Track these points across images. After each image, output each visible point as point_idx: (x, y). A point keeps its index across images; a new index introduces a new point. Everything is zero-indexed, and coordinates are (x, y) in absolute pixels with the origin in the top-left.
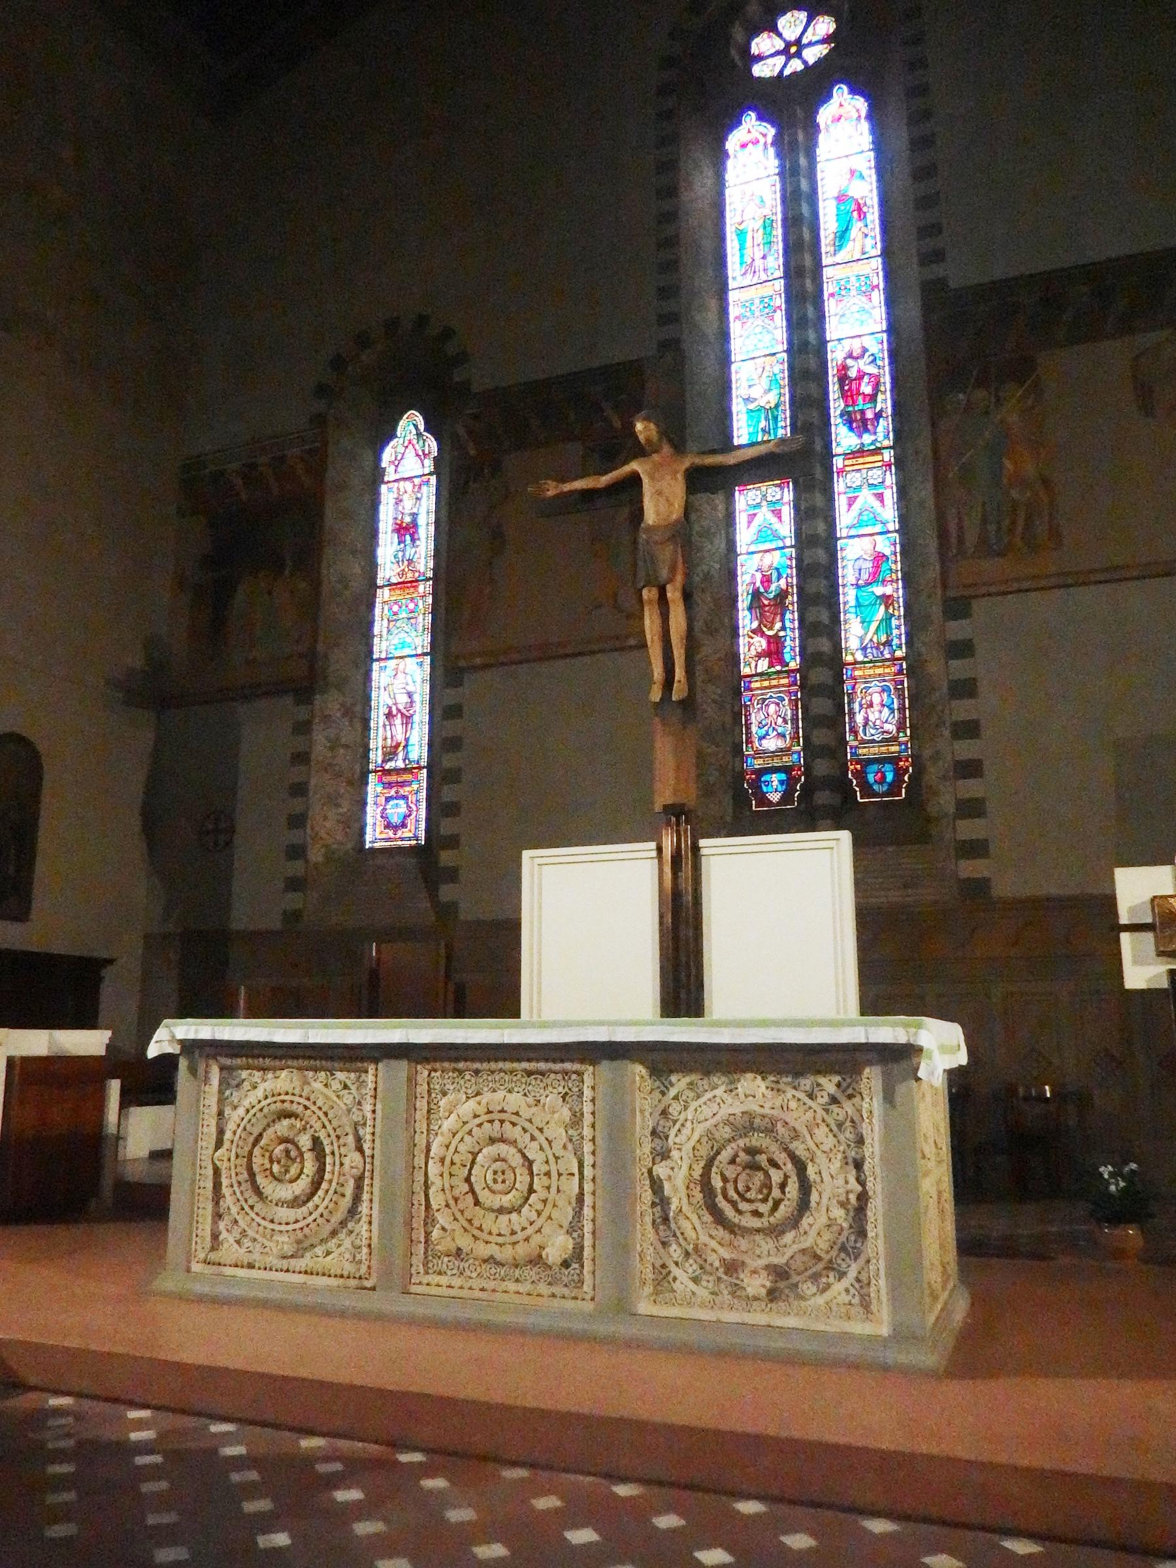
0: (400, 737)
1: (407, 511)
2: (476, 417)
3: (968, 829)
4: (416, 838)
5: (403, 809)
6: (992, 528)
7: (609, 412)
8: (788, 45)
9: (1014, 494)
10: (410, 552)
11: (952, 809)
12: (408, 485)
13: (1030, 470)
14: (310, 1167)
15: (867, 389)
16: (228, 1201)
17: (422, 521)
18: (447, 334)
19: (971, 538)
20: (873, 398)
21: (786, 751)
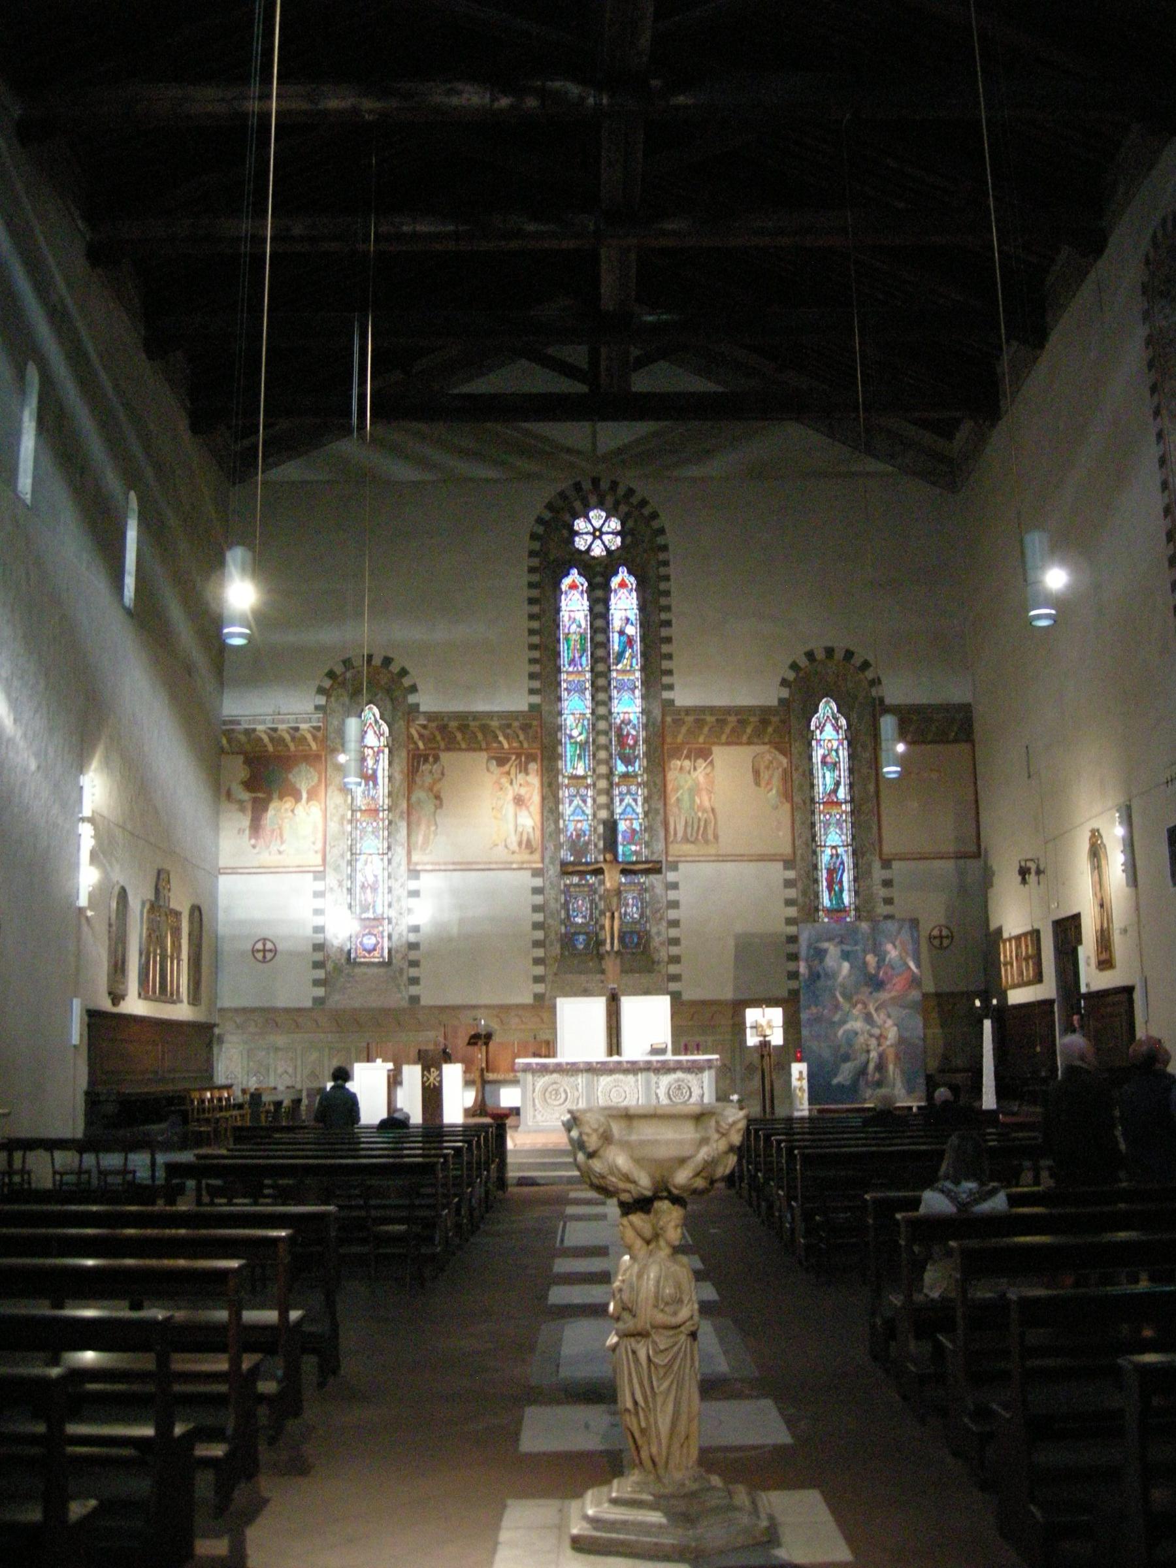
0: (370, 900)
1: (370, 766)
2: (424, 727)
3: (673, 969)
4: (382, 956)
5: (373, 941)
6: (689, 830)
7: (501, 738)
9: (700, 814)
10: (372, 792)
11: (666, 959)
12: (370, 751)
13: (707, 804)
14: (563, 1096)
15: (631, 742)
16: (538, 1106)
17: (380, 774)
18: (404, 672)
19: (680, 834)
20: (633, 747)
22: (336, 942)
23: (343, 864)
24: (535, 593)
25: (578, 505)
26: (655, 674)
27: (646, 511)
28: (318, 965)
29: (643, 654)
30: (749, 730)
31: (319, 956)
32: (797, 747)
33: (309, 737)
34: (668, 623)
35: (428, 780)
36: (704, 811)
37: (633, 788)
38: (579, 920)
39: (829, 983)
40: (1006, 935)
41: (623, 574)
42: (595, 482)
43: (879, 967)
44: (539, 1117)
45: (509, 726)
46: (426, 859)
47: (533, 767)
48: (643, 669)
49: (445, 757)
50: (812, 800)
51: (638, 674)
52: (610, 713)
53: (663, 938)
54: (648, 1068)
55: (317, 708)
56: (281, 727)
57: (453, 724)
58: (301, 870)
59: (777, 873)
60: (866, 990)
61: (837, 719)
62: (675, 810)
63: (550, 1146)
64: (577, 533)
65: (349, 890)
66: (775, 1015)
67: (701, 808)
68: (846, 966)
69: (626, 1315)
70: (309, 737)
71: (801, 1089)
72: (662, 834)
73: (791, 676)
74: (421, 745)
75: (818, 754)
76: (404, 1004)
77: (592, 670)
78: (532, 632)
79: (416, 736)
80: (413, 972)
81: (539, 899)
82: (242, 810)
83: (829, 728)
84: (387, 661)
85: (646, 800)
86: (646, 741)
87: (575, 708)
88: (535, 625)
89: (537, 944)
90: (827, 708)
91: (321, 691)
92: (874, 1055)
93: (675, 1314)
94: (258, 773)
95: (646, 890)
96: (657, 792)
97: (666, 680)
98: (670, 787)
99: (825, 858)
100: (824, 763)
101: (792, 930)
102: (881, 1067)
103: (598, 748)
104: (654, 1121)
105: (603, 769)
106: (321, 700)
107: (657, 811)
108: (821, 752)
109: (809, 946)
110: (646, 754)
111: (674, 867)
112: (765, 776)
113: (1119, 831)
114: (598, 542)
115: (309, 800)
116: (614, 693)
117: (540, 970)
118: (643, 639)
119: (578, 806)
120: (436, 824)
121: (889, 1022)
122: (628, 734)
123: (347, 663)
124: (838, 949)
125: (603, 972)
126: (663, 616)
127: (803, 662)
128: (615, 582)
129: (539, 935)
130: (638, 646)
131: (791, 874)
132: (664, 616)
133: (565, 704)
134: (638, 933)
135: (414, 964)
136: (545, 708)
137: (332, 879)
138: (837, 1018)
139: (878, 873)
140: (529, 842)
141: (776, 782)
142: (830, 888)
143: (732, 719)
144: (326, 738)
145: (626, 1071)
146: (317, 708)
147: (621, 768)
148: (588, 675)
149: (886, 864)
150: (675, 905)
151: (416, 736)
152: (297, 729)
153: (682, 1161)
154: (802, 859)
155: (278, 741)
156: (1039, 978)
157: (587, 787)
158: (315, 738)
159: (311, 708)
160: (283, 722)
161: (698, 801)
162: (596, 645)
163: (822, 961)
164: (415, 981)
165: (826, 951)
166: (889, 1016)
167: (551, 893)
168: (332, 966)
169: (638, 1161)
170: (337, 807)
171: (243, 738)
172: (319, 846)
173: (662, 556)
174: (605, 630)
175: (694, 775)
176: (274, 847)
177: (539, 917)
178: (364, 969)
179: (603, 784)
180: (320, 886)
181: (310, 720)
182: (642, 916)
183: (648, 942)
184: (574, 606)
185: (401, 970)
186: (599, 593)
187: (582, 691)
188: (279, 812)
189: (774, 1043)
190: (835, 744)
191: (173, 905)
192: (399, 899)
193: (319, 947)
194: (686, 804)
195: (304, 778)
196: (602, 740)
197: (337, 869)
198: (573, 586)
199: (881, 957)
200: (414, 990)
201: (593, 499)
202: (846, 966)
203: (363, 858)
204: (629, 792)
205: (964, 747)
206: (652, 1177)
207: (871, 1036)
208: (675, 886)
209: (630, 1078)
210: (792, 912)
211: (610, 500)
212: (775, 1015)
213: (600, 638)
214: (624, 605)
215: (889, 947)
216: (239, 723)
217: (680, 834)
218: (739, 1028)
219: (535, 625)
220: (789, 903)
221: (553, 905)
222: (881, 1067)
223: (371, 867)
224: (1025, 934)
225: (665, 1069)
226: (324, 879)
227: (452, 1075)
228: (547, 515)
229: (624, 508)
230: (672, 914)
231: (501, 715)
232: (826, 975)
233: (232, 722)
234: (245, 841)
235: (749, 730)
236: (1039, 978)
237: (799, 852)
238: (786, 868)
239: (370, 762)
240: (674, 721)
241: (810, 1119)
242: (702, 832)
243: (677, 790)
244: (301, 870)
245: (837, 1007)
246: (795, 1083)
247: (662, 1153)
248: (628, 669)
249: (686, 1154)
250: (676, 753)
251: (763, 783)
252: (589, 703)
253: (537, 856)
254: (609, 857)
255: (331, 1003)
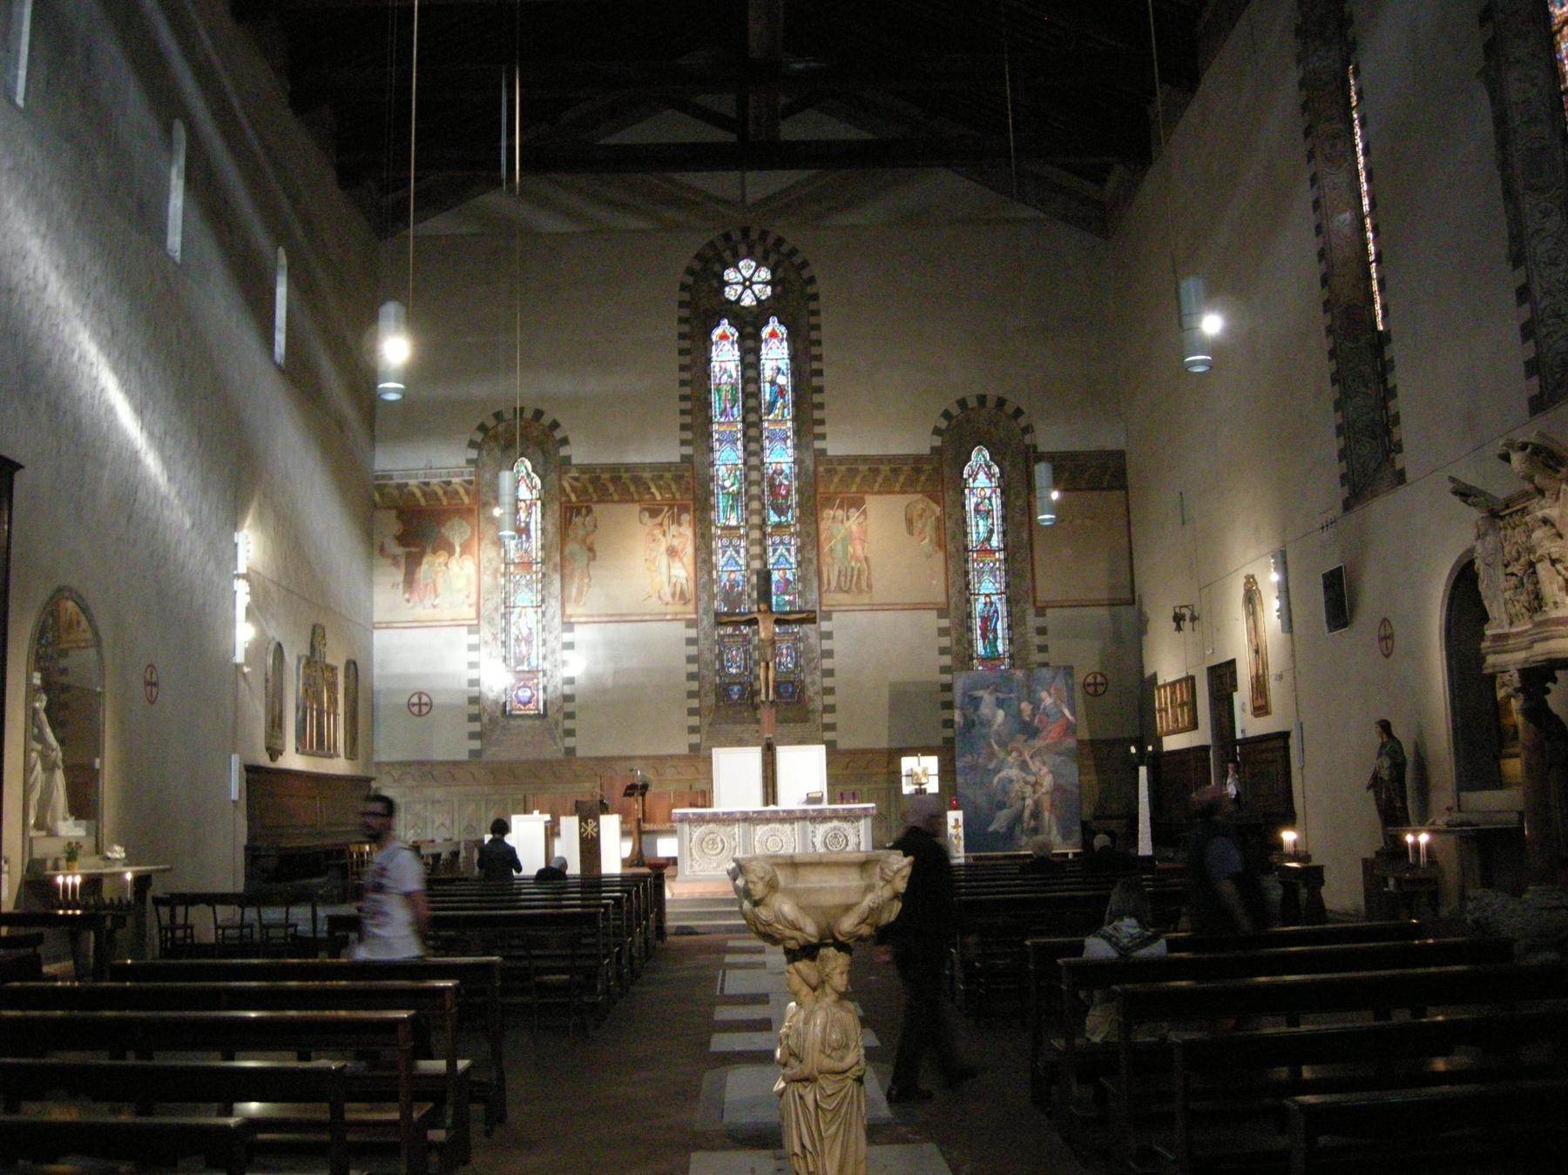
2: (576, 479)
3: (828, 718)
5: (528, 693)
7: (653, 490)
8: (745, 280)
13: (860, 553)
16: (695, 856)
17: (532, 527)
18: (555, 425)
19: (834, 584)
21: (741, 674)
22: (491, 696)
23: (498, 617)
24: (686, 344)
25: (727, 255)
26: (806, 424)
27: (797, 260)
28: (473, 718)
29: (795, 404)
30: (902, 478)
31: (475, 709)
32: (950, 496)
33: (462, 491)
34: (819, 373)
35: (581, 532)
36: (857, 560)
37: (786, 539)
38: (733, 670)
39: (984, 731)
40: (1160, 682)
41: (773, 324)
42: (745, 232)
43: (1033, 716)
44: (696, 867)
45: (661, 477)
46: (580, 610)
47: (686, 518)
48: (794, 419)
49: (597, 508)
50: (966, 549)
51: (789, 424)
52: (763, 463)
53: (817, 688)
54: (803, 817)
55: (469, 462)
56: (434, 481)
57: (605, 476)
58: (456, 624)
59: (931, 620)
60: (1021, 737)
61: (989, 467)
62: (828, 560)
63: (708, 896)
64: (727, 284)
65: (504, 643)
66: (931, 763)
67: (855, 557)
68: (1001, 714)
69: (792, 1061)
70: (462, 491)
71: (957, 836)
72: (816, 584)
73: (943, 424)
74: (573, 498)
75: (971, 502)
76: (560, 755)
77: (744, 421)
78: (683, 383)
79: (568, 489)
80: (568, 724)
81: (693, 650)
82: (396, 563)
83: (981, 476)
84: (539, 414)
85: (799, 550)
86: (798, 491)
87: (727, 458)
88: (686, 376)
89: (691, 695)
90: (980, 456)
91: (472, 444)
92: (1029, 802)
93: (842, 1059)
94: (410, 527)
95: (800, 640)
96: (810, 542)
97: (818, 429)
98: (823, 537)
99: (979, 606)
100: (977, 511)
101: (947, 678)
102: (1036, 815)
103: (751, 498)
104: (819, 869)
105: (756, 520)
106: (473, 454)
107: (810, 560)
108: (974, 500)
109: (964, 694)
110: (799, 505)
111: (828, 616)
112: (918, 525)
113: (1275, 577)
114: (748, 292)
115: (462, 553)
116: (767, 443)
117: (695, 721)
118: (794, 389)
119: (731, 557)
120: (589, 577)
121: (1045, 770)
122: (781, 484)
123: (498, 416)
124: (993, 698)
125: (758, 721)
126: (815, 365)
127: (955, 411)
128: (765, 332)
129: (694, 686)
130: (789, 396)
131: (945, 623)
132: (815, 365)
133: (717, 455)
134: (792, 683)
135: (570, 716)
136: (697, 459)
137: (486, 632)
138: (991, 766)
139: (1032, 621)
140: (682, 593)
141: (929, 531)
142: (984, 636)
143: (885, 468)
144: (478, 492)
145: (782, 820)
146: (469, 462)
147: (774, 518)
148: (740, 426)
149: (1040, 611)
150: (829, 654)
151: (568, 489)
152: (449, 483)
153: (848, 908)
154: (957, 607)
155: (429, 494)
156: (1194, 725)
157: (740, 537)
158: (468, 492)
159: (463, 462)
160: (434, 476)
161: (851, 550)
162: (746, 395)
163: (977, 708)
164: (570, 733)
165: (980, 699)
166: (1044, 763)
167: (705, 644)
168: (488, 719)
169: (803, 909)
170: (489, 560)
171: (395, 492)
172: (473, 599)
173: (812, 305)
174: (757, 380)
175: (847, 524)
176: (428, 602)
177: (694, 668)
178: (520, 721)
179: (756, 534)
180: (474, 639)
181: (462, 474)
182: (796, 666)
183: (802, 691)
184: (725, 357)
185: (557, 723)
186: (750, 343)
187: (734, 442)
188: (432, 566)
189: (929, 791)
190: (988, 492)
191: (329, 660)
192: (553, 652)
193: (474, 700)
194: (839, 553)
195: (457, 533)
196: (755, 490)
197: (491, 621)
198: (724, 337)
199: (1036, 705)
200: (570, 742)
201: (743, 249)
202: (1001, 714)
203: (517, 610)
204: (782, 543)
205: (1119, 493)
206: (818, 924)
207: (1027, 783)
208: (828, 635)
209: (787, 827)
210: (947, 660)
211: (759, 250)
212: (931, 763)
213: (751, 388)
214: (775, 355)
215: (1044, 694)
216: (391, 478)
217: (834, 584)
218: (895, 775)
219: (686, 376)
220: (943, 651)
221: (708, 656)
222: (1036, 815)
223: (526, 620)
224: (1179, 681)
225: (821, 817)
226: (478, 632)
227: (610, 826)
228: (697, 266)
229: (773, 258)
230: (827, 663)
231: (652, 466)
232: (982, 724)
233: (383, 477)
234: (399, 594)
235: (902, 478)
236: (1194, 725)
237: (953, 601)
238: (940, 617)
239: (523, 515)
240: (828, 471)
241: (967, 866)
242: (855, 581)
243: (829, 539)
244: (456, 624)
245: (992, 755)
246: (951, 830)
247: (828, 900)
248: (780, 420)
249: (852, 900)
250: (829, 502)
251: (916, 532)
252: (740, 453)
253: (690, 607)
254: (763, 607)
255: (486, 757)
